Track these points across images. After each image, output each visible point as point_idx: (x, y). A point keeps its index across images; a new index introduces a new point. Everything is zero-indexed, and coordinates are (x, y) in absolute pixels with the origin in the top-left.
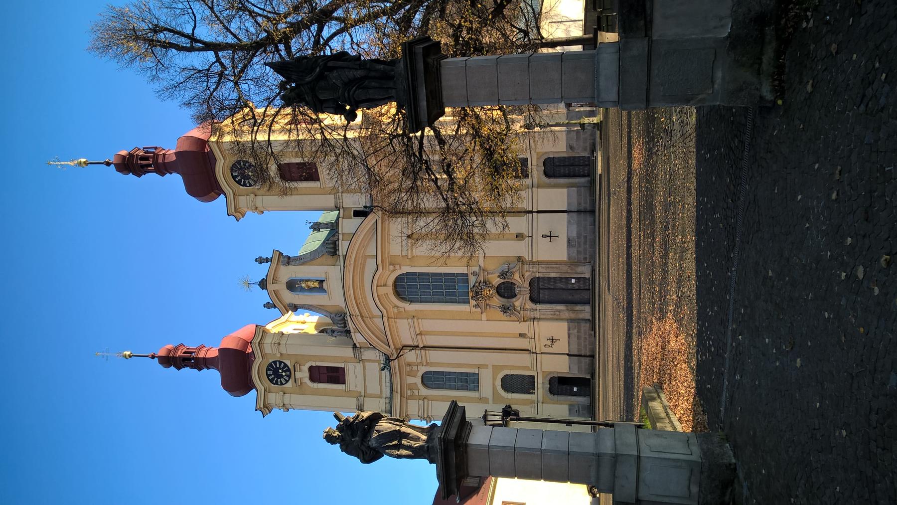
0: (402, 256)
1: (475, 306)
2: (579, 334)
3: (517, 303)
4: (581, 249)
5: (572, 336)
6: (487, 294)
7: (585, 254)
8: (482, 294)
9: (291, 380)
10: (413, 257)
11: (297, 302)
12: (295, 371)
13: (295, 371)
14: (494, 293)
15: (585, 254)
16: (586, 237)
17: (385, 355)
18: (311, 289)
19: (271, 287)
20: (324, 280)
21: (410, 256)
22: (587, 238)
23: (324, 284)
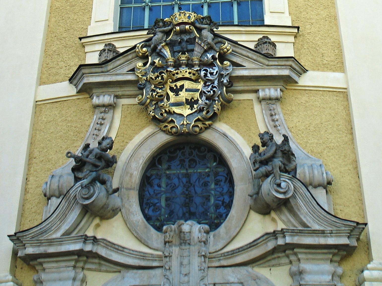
6: (176, 91)
8: (177, 65)
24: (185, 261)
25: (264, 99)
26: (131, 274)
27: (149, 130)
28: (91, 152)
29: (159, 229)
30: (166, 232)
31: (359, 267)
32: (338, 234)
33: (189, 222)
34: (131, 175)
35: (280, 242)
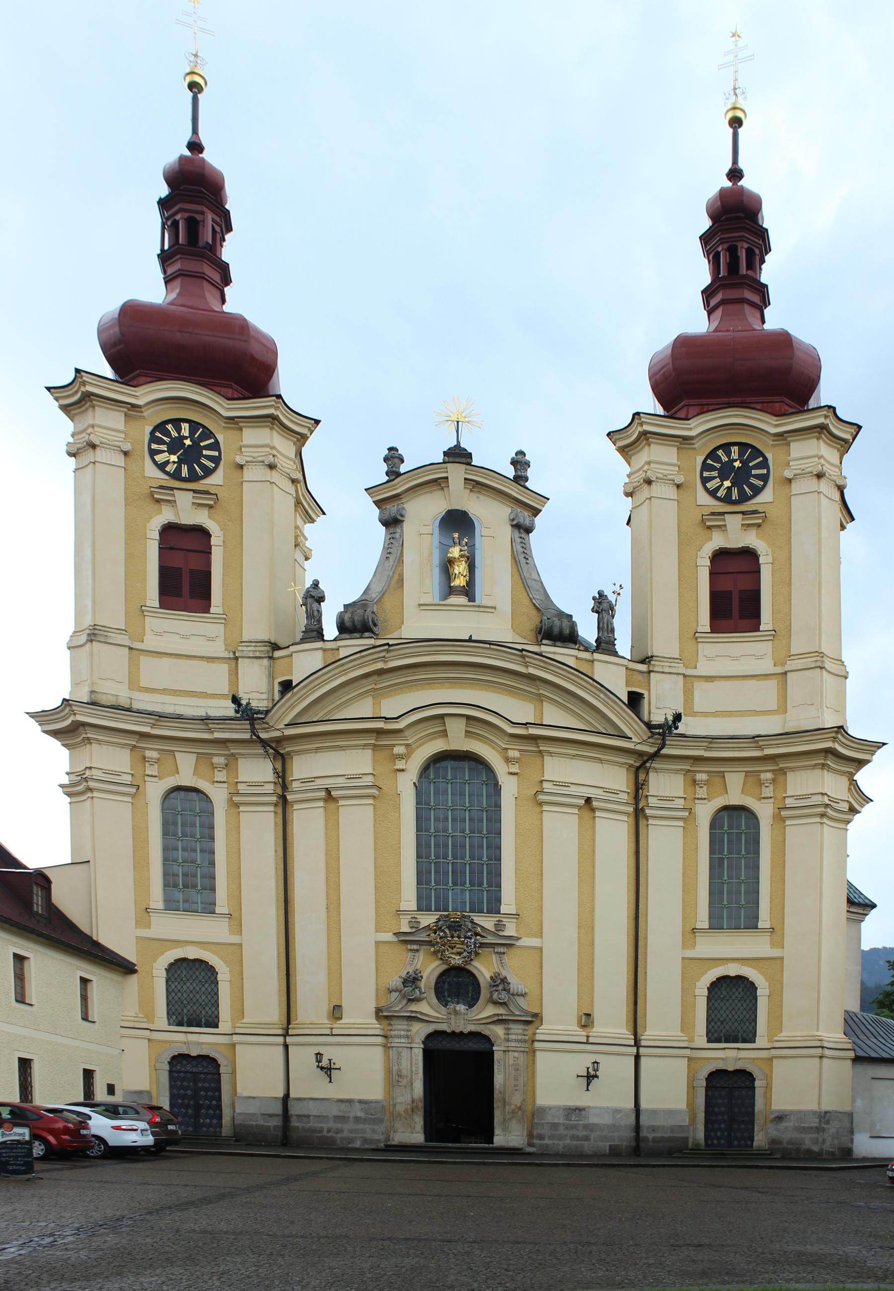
0: (542, 782)
1: (414, 923)
2: (351, 1119)
3: (428, 1007)
4: (562, 1131)
5: (343, 1107)
7: (551, 1137)
9: (166, 477)
10: (541, 804)
11: (408, 528)
12: (195, 491)
13: (195, 491)
14: (453, 962)
15: (551, 1137)
16: (587, 1138)
17: (267, 712)
18: (447, 565)
19: (456, 473)
20: (472, 599)
21: (541, 797)
22: (586, 1140)
23: (463, 600)
24: (457, 1022)
25: (497, 952)
26: (432, 1024)
27: (438, 962)
28: (411, 976)
29: (445, 1006)
30: (448, 1009)
31: (537, 1026)
32: (527, 1016)
33: (459, 1005)
34: (430, 983)
35: (500, 1018)
